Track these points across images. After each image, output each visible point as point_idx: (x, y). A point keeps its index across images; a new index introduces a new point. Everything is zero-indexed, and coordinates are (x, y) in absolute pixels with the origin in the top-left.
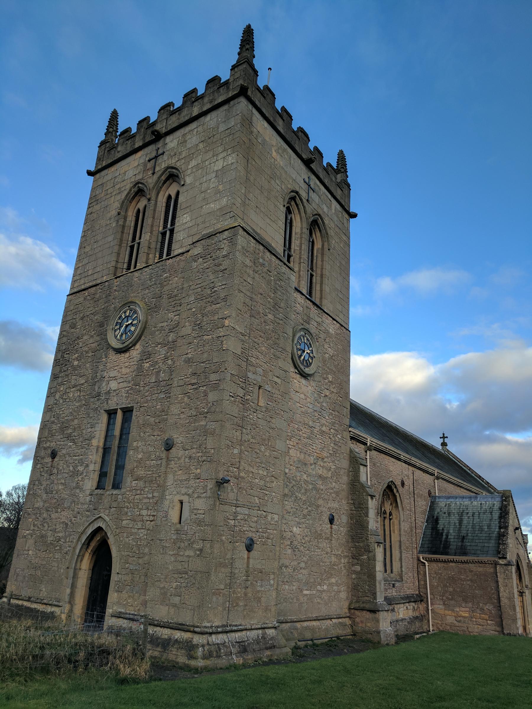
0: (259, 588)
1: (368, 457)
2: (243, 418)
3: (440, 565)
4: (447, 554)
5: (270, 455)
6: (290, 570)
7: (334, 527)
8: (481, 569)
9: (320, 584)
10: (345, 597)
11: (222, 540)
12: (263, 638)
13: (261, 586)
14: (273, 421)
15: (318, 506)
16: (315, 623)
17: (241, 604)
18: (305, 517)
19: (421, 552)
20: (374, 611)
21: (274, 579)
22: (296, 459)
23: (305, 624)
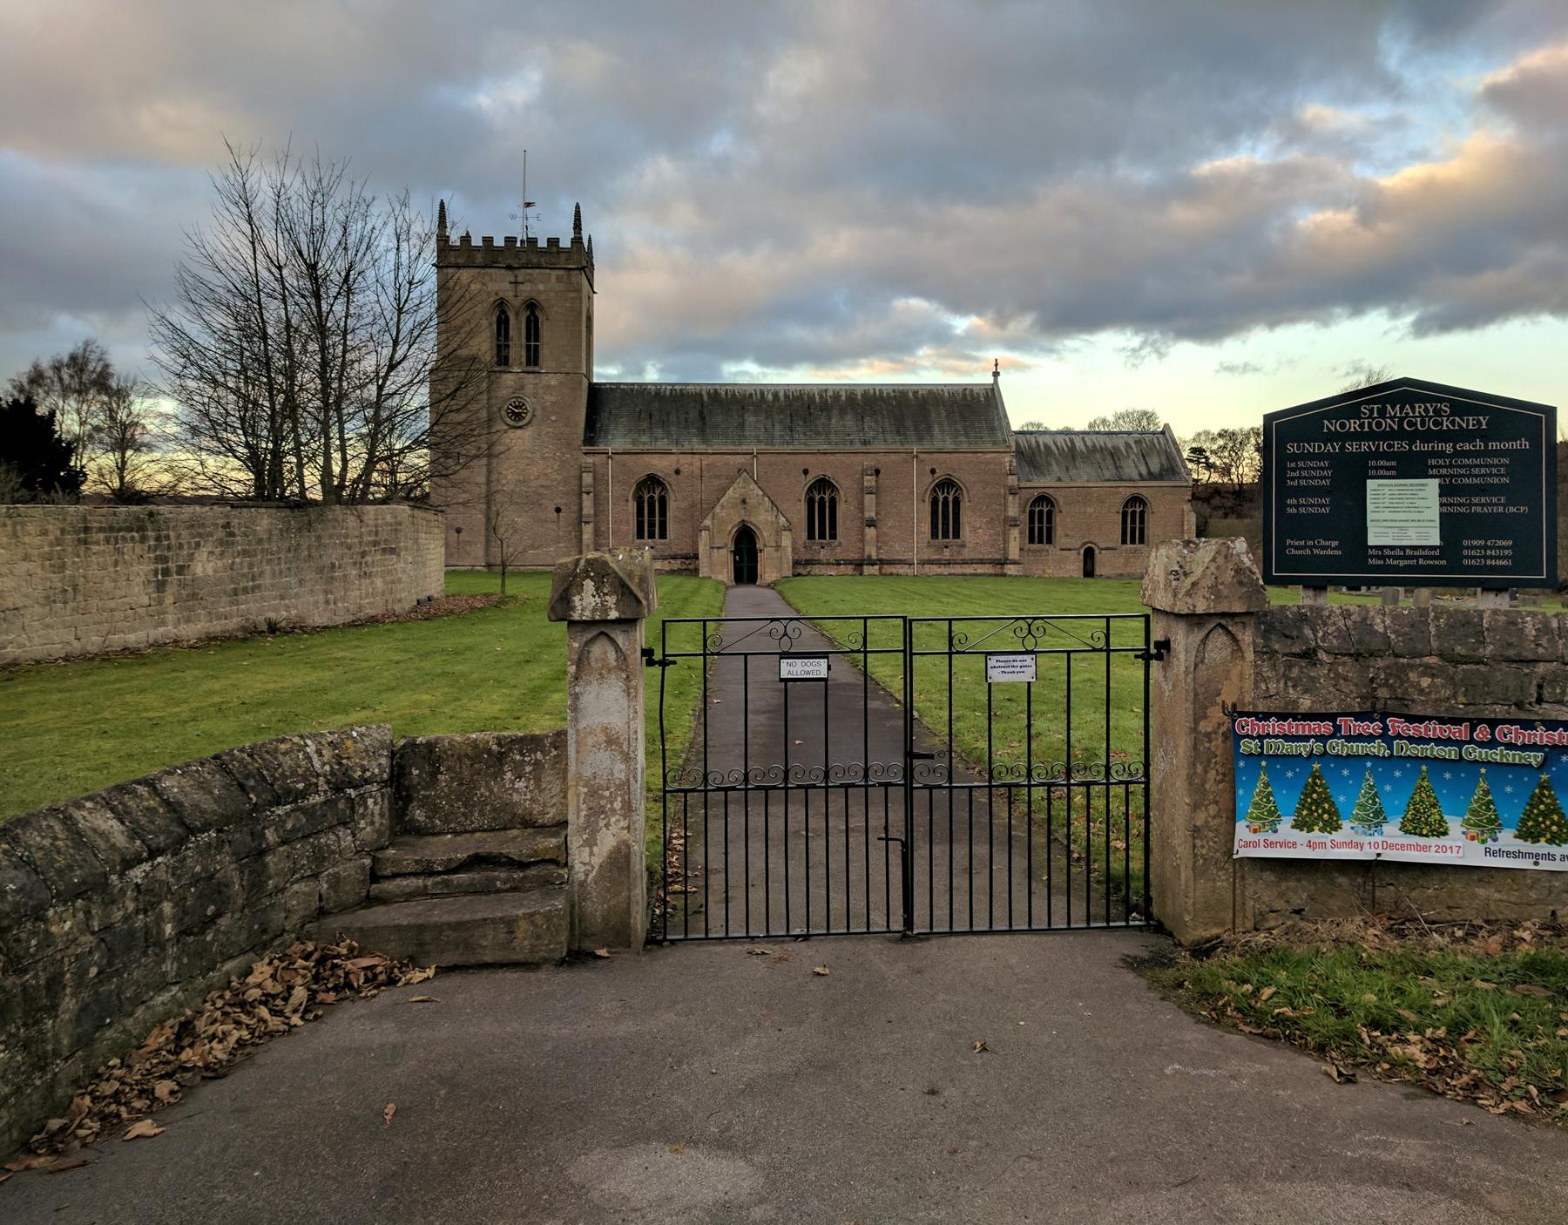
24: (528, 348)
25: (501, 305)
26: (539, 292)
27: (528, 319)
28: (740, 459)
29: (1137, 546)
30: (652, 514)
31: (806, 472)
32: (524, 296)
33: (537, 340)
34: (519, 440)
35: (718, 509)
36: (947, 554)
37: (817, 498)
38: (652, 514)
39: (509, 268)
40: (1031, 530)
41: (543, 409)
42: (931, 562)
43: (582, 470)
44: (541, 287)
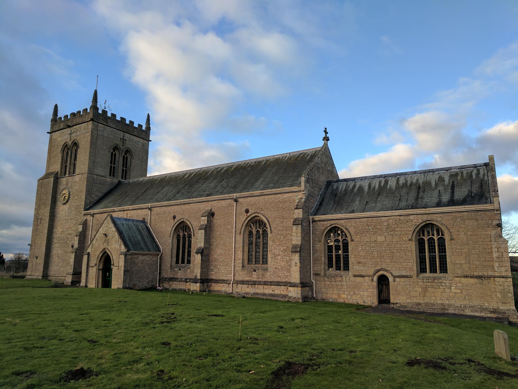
25: (65, 146)
29: (438, 274)
31: (174, 217)
32: (73, 139)
36: (255, 277)
37: (181, 235)
39: (69, 127)
40: (330, 258)
42: (243, 282)
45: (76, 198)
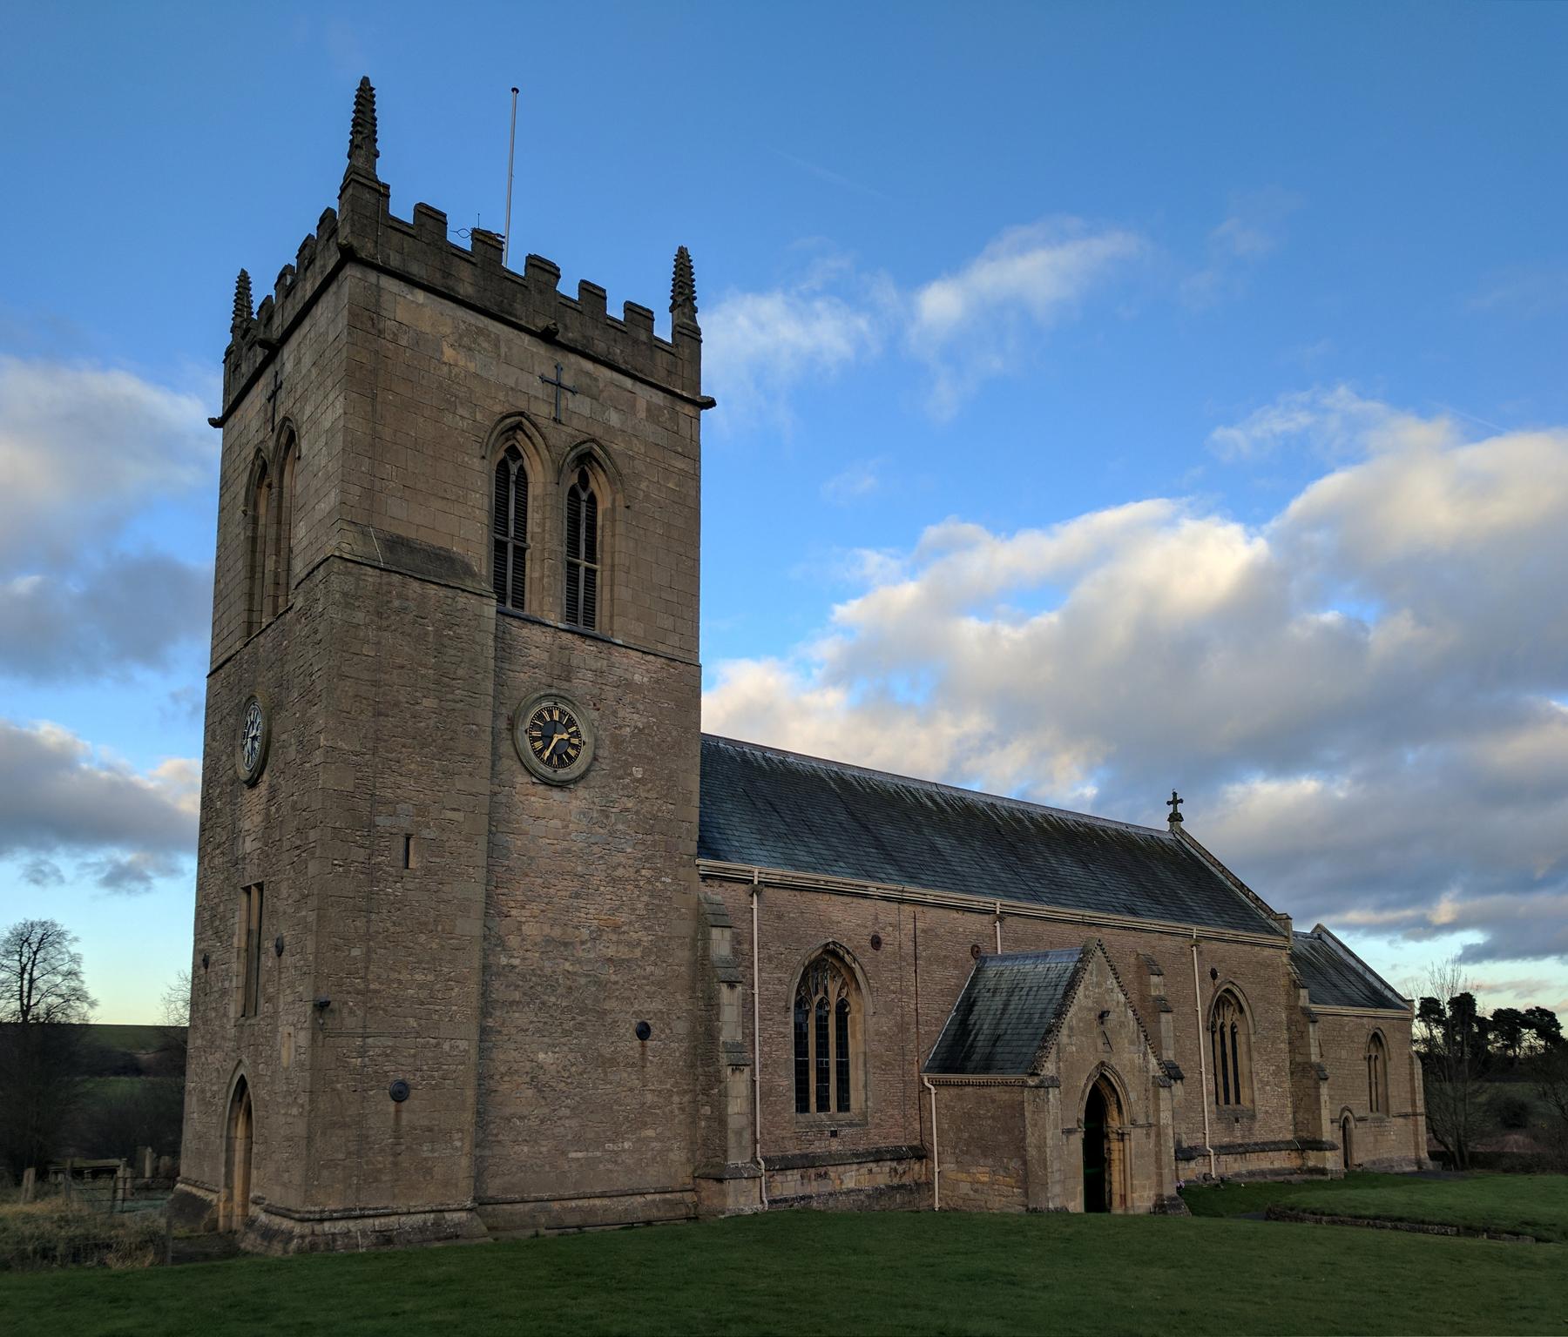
0: (425, 1155)
1: (755, 906)
2: (369, 897)
3: (953, 1091)
4: (962, 1071)
5: (443, 947)
6: (534, 1123)
7: (649, 1043)
8: (1006, 1097)
9: (614, 1142)
10: (683, 1160)
11: (334, 1090)
12: (436, 1224)
13: (433, 1151)
14: (446, 888)
15: (603, 1014)
16: (597, 1202)
17: (385, 1178)
18: (566, 1033)
19: (929, 1069)
20: (720, 1180)
21: (461, 1139)
22: (539, 939)
23: (573, 1204)
24: (572, 567)
26: (609, 429)
27: (573, 493)
28: (974, 923)
30: (822, 1050)
33: (591, 556)
34: (550, 818)
35: (1063, 1037)
38: (822, 1050)
41: (617, 743)
43: (707, 919)
44: (614, 418)
45: (638, 772)
